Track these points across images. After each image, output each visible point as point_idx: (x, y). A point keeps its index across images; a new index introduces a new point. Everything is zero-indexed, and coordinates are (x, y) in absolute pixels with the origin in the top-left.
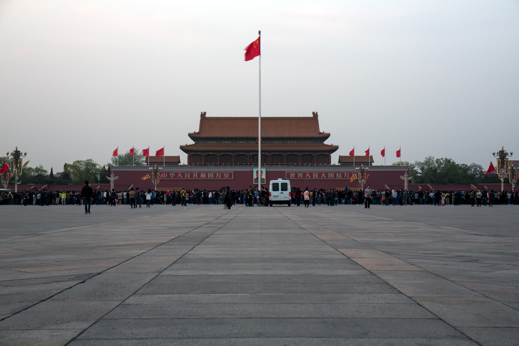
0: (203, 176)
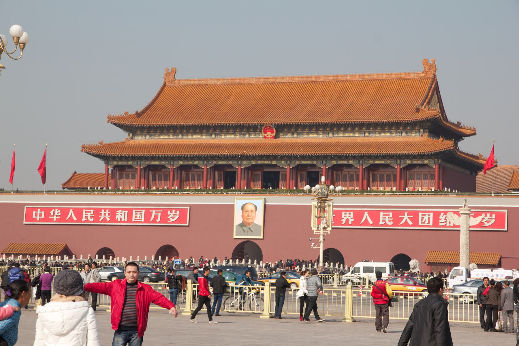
0: (121, 216)
